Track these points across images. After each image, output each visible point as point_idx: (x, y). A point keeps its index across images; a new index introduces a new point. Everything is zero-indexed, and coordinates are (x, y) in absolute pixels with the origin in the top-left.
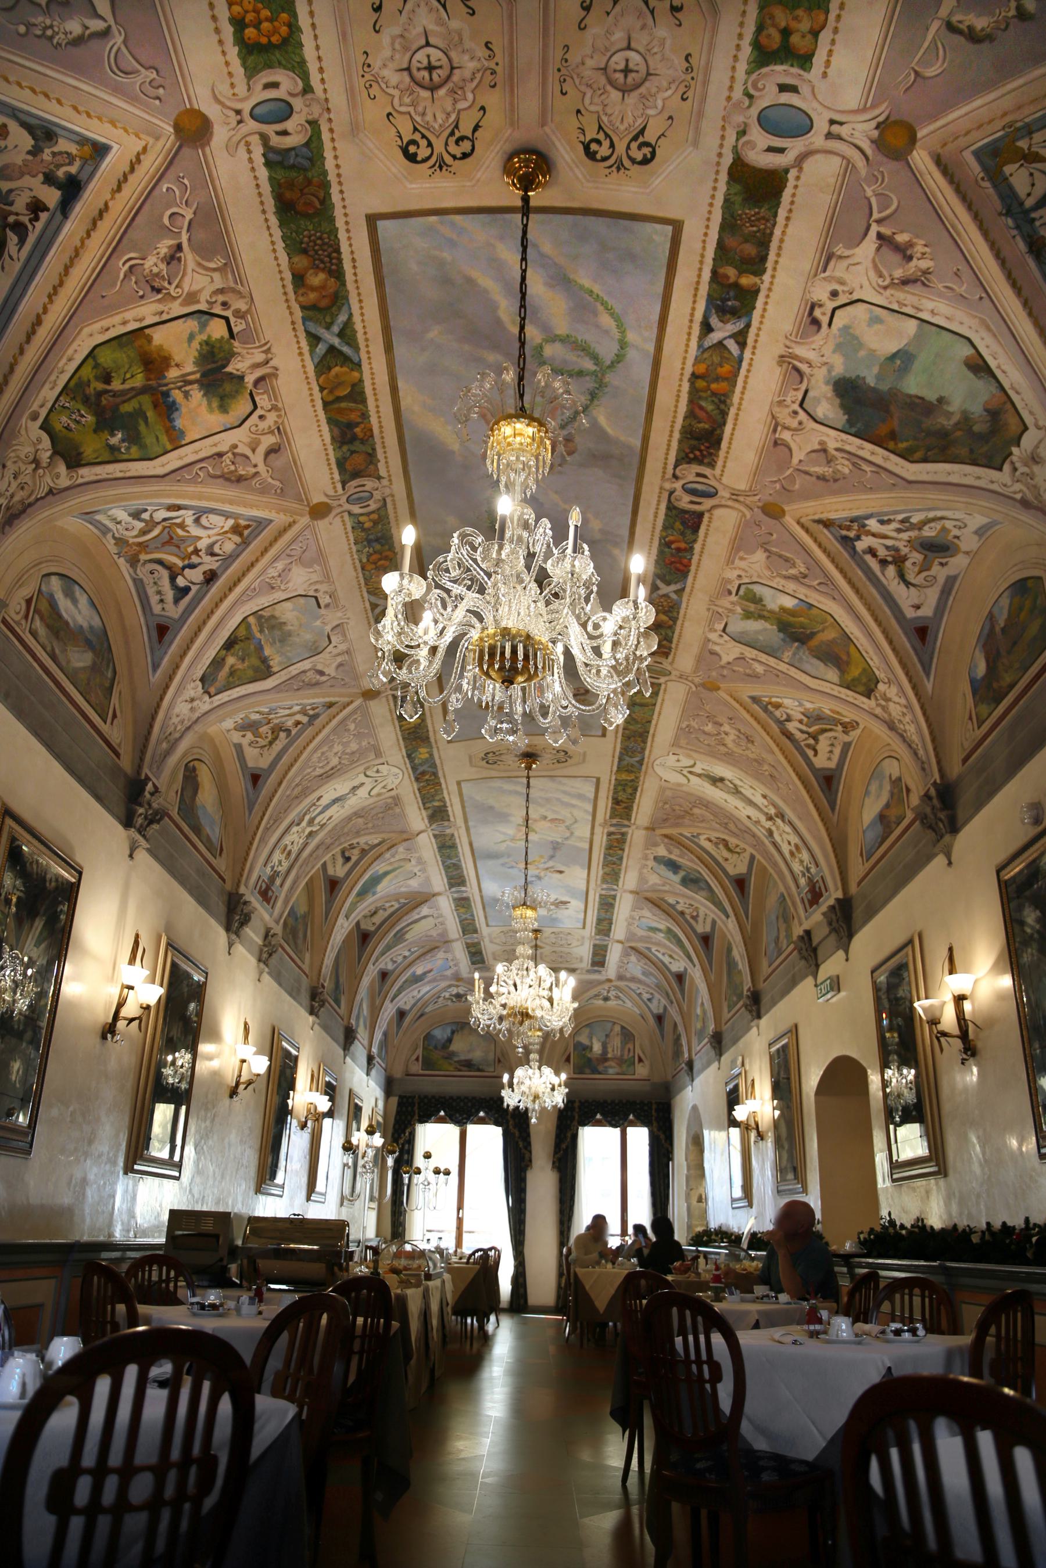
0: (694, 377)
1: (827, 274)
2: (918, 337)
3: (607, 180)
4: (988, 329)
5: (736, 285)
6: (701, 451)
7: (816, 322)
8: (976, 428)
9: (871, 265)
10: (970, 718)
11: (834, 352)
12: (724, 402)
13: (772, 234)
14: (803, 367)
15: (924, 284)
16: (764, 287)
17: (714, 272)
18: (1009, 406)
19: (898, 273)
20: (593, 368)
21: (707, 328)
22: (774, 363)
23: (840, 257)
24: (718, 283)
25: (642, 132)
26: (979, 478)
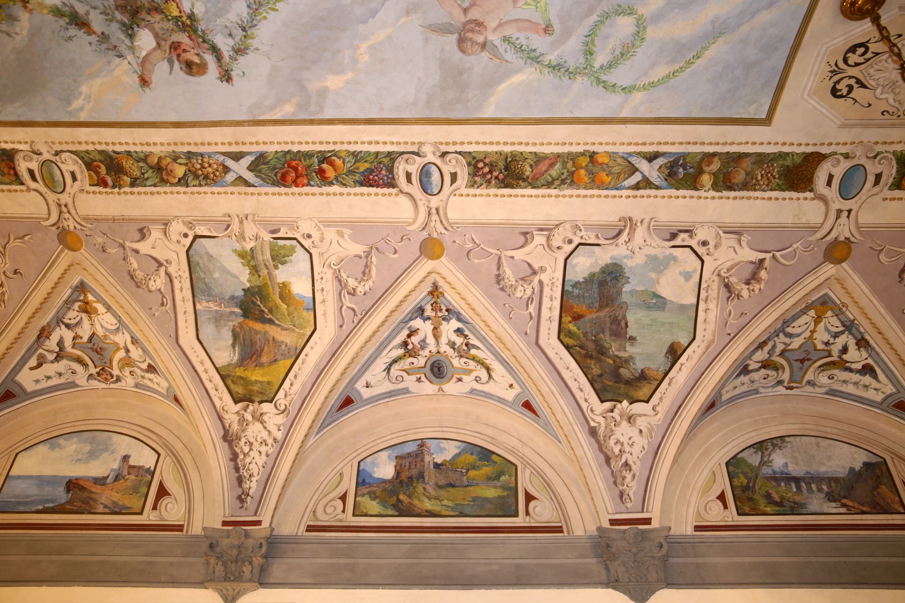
0: (592, 155)
1: (723, 235)
2: (682, 308)
3: (825, 61)
4: (707, 348)
5: (701, 172)
6: (490, 172)
7: (674, 236)
8: (623, 371)
9: (736, 261)
10: (343, 498)
11: (646, 256)
12: (563, 182)
13: (755, 190)
14: (624, 237)
15: (728, 298)
16: (702, 193)
17: (714, 155)
18: (656, 383)
19: (733, 280)
20: (597, 65)
21: (651, 158)
22: (621, 215)
23: (739, 240)
24: (702, 160)
25: (863, 86)
26: (581, 390)
